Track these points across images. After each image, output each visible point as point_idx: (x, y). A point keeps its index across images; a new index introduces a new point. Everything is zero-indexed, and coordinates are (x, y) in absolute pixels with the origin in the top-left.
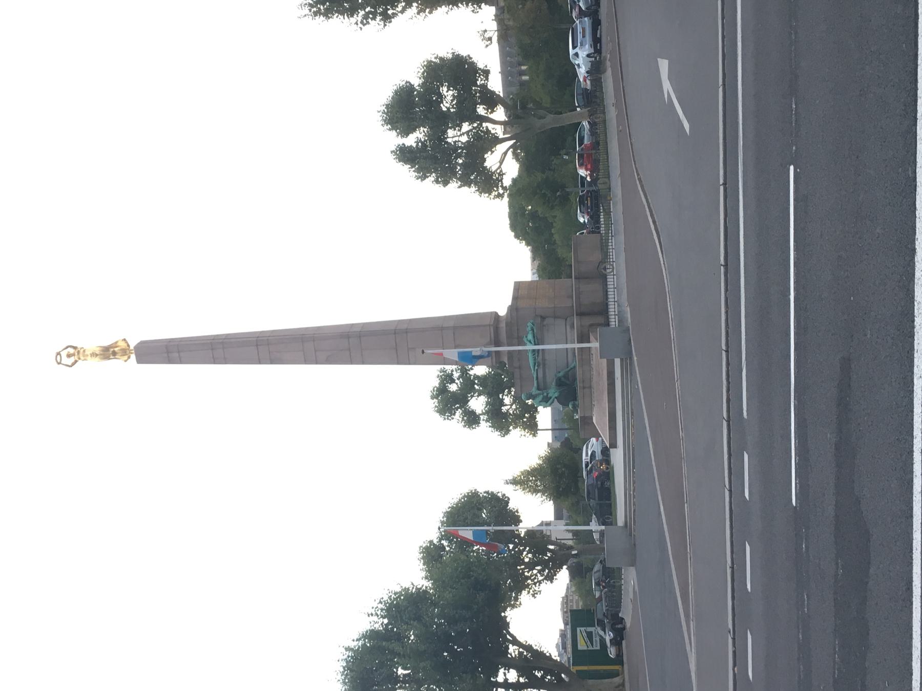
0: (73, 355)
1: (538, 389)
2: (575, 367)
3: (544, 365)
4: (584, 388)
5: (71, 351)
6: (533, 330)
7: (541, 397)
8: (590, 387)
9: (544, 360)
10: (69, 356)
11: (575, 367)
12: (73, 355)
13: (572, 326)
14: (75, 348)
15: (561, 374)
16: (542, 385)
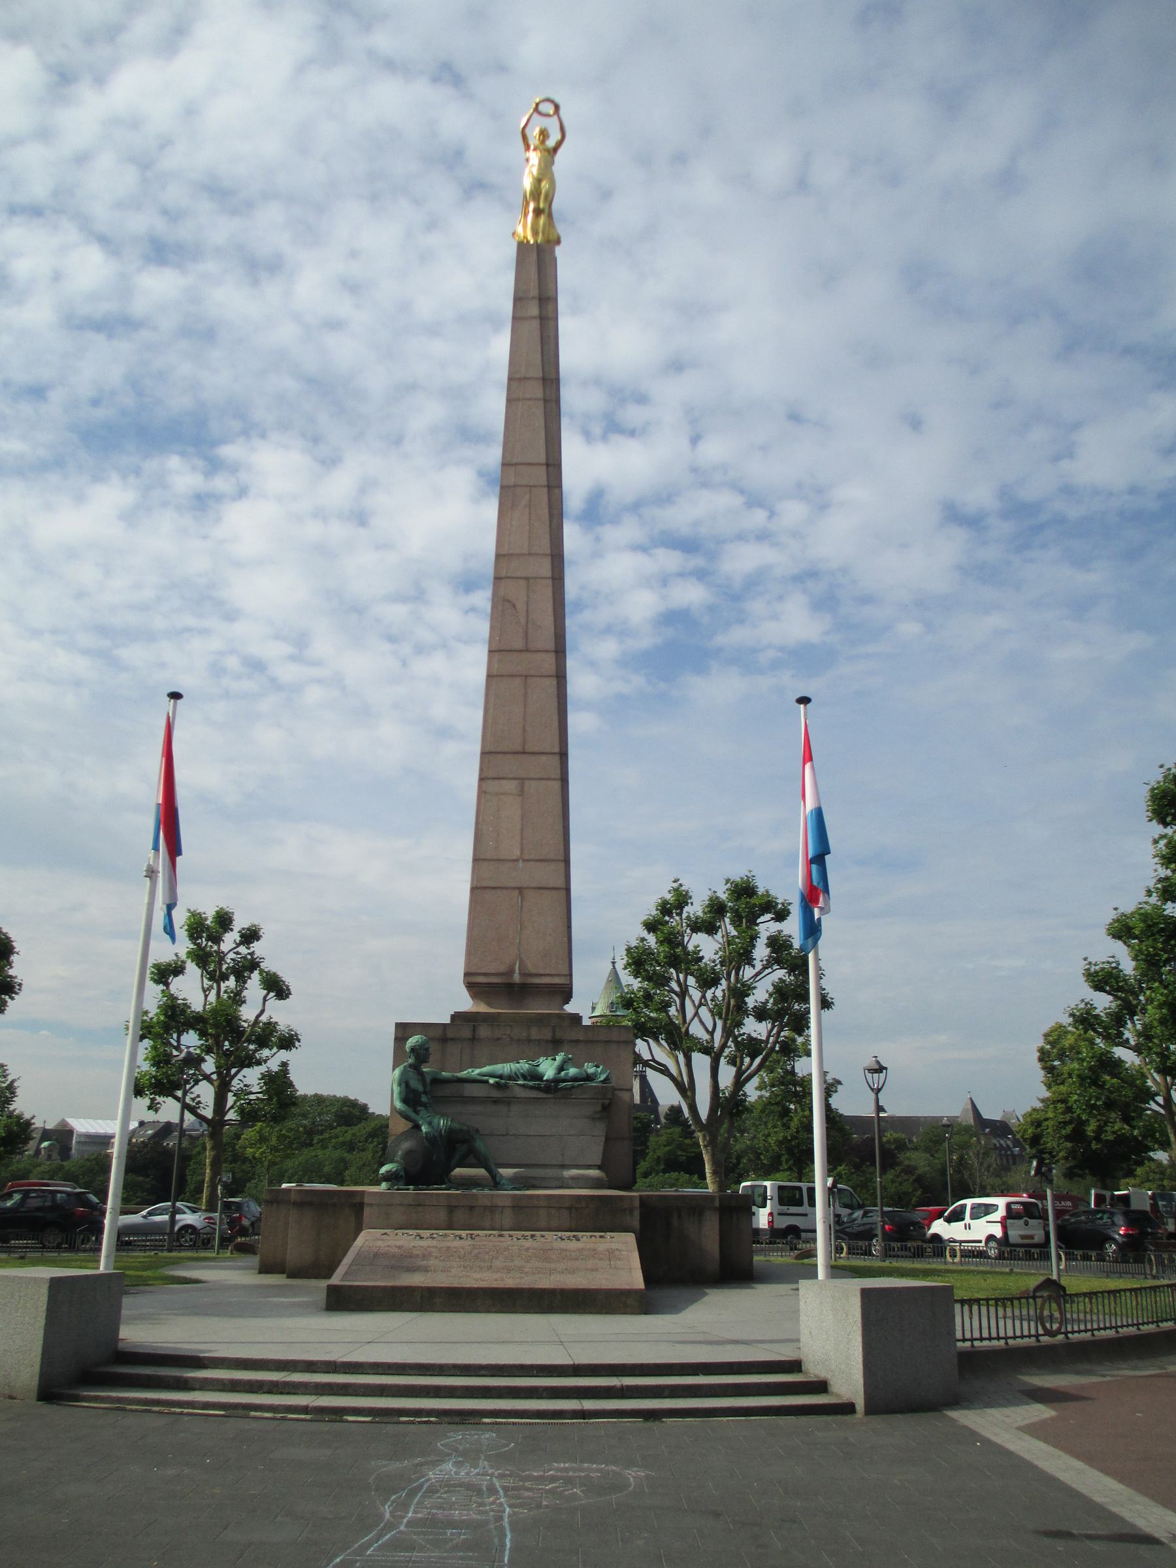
0: (543, 142)
1: (437, 1081)
2: (496, 1183)
3: (496, 1101)
4: (451, 1209)
5: (551, 143)
6: (589, 1078)
7: (416, 1084)
8: (450, 1227)
9: (508, 1102)
10: (544, 134)
11: (496, 1183)
12: (543, 142)
13: (597, 1184)
14: (555, 150)
15: (480, 1145)
16: (448, 1090)
